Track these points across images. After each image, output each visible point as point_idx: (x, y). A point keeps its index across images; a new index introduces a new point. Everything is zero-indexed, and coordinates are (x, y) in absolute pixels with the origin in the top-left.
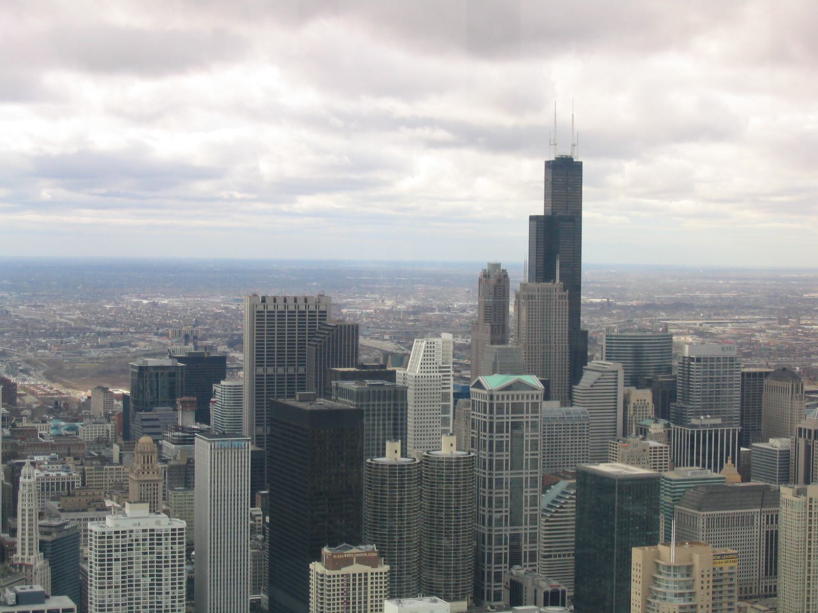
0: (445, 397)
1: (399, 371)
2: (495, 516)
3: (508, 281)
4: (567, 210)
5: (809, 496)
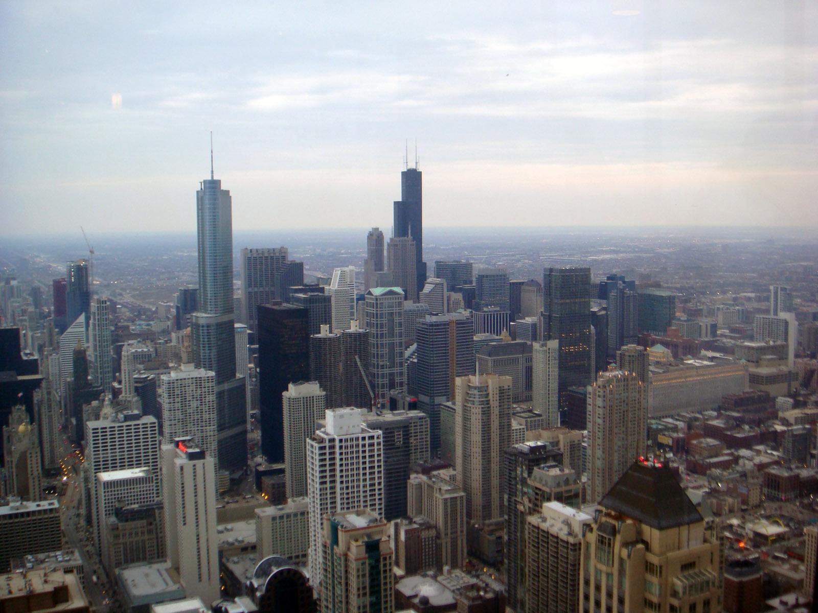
1: (326, 287)
2: (381, 363)
5: (548, 347)
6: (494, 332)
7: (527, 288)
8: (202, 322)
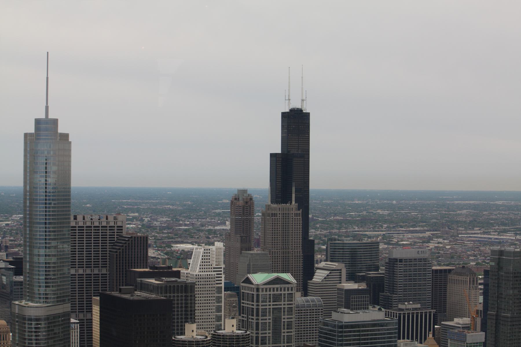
0: (219, 290)
1: (183, 271)
3: (252, 204)
4: (298, 149)
6: (417, 338)
7: (456, 277)
8: (32, 313)
